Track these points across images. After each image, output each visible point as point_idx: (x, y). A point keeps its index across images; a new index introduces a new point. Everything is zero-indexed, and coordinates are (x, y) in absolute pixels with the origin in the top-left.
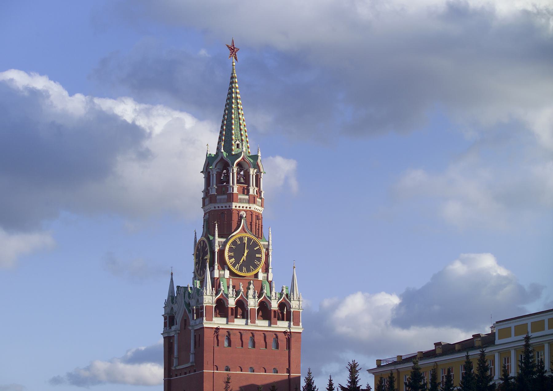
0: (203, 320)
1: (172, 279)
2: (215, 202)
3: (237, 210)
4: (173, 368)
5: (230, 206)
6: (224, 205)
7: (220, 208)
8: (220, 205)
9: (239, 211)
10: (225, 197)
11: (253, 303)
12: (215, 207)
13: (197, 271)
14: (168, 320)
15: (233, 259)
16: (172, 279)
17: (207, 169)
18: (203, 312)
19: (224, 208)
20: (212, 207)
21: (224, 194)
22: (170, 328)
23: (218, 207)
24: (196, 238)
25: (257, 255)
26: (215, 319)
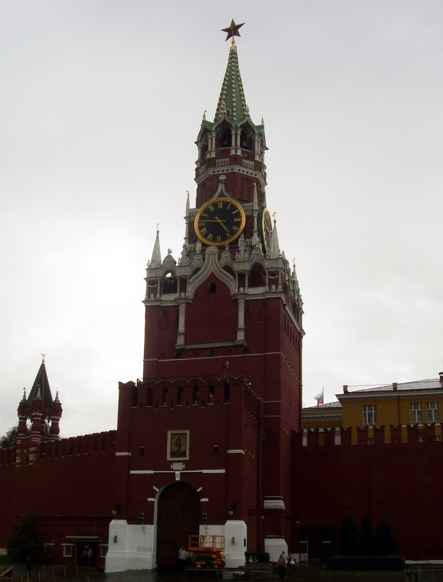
0: (277, 288)
1: (158, 238)
2: (241, 164)
5: (256, 175)
6: (250, 171)
8: (246, 170)
10: (253, 163)
12: (239, 170)
13: (205, 236)
16: (158, 238)
17: (216, 129)
19: (249, 175)
20: (236, 169)
22: (160, 296)
23: (243, 171)
24: (188, 200)
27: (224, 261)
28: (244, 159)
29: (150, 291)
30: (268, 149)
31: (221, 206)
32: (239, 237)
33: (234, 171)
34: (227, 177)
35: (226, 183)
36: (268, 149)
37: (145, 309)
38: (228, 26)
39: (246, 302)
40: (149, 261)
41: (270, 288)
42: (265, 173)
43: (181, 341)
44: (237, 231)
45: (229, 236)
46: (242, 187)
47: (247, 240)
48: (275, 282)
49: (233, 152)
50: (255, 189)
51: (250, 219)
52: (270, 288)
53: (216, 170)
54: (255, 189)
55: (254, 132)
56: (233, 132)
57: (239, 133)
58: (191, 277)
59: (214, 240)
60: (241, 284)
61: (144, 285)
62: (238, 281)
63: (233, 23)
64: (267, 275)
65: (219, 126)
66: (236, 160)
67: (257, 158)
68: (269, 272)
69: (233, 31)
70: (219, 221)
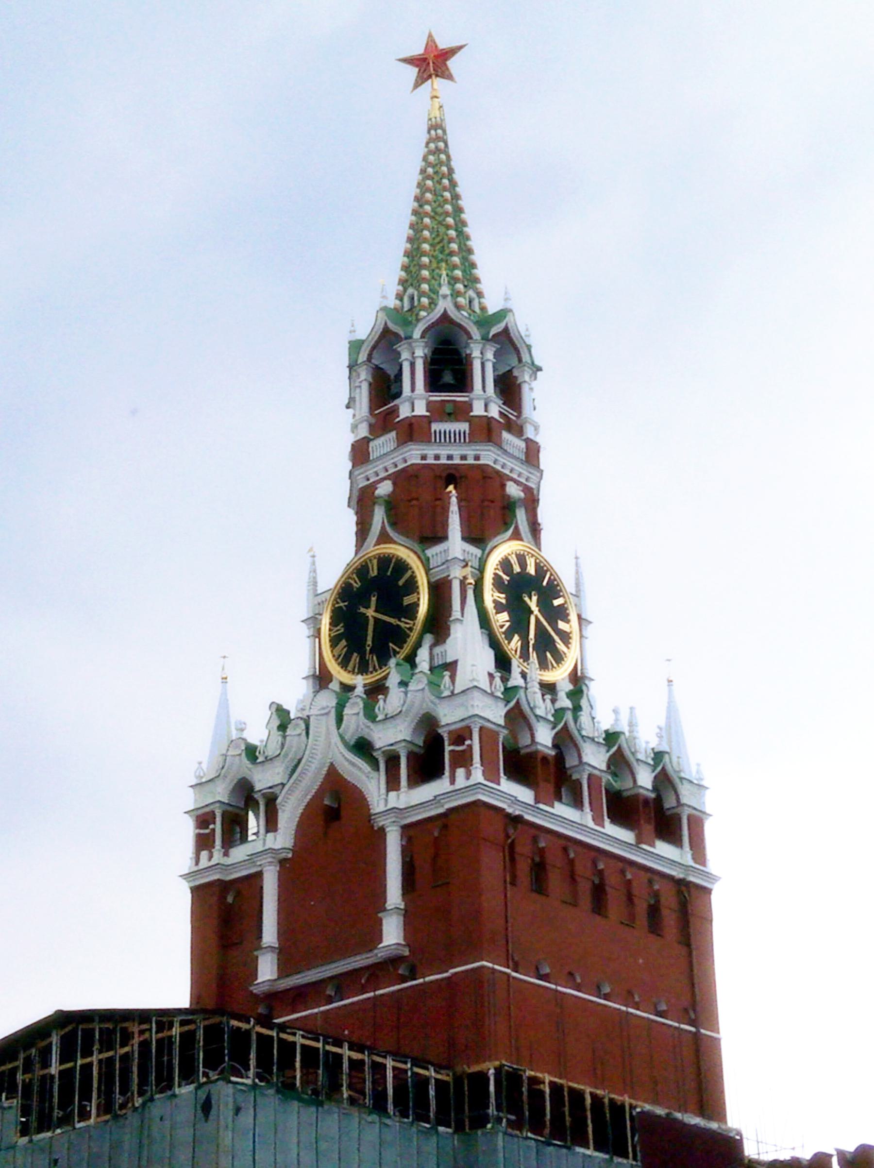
0: (468, 775)
1: (224, 693)
3: (498, 472)
4: (255, 990)
5: (477, 458)
6: (456, 452)
7: (443, 461)
8: (444, 452)
9: (501, 479)
10: (464, 427)
11: (595, 758)
13: (344, 663)
14: (218, 827)
15: (504, 616)
17: (370, 358)
18: (470, 747)
19: (457, 461)
20: (414, 454)
21: (457, 420)
22: (226, 854)
25: (562, 625)
26: (503, 779)
27: (353, 727)
28: (436, 421)
29: (203, 843)
30: (539, 369)
31: (374, 572)
32: (418, 645)
33: (409, 463)
34: (395, 484)
35: (392, 505)
36: (539, 369)
37: (190, 895)
38: (418, 49)
39: (406, 828)
40: (200, 763)
41: (453, 781)
42: (528, 441)
43: (267, 970)
44: (411, 629)
45: (394, 650)
46: (437, 499)
47: (438, 650)
48: (463, 760)
49: (404, 412)
50: (454, 500)
51: (440, 591)
52: (453, 781)
53: (370, 473)
54: (454, 500)
55: (471, 338)
56: (405, 355)
57: (420, 352)
58: (283, 785)
59: (363, 669)
60: (393, 784)
61: (186, 832)
62: (387, 773)
63: (431, 40)
64: (446, 743)
65: (374, 348)
66: (413, 431)
67: (478, 410)
68: (450, 732)
69: (432, 63)
70: (370, 613)
